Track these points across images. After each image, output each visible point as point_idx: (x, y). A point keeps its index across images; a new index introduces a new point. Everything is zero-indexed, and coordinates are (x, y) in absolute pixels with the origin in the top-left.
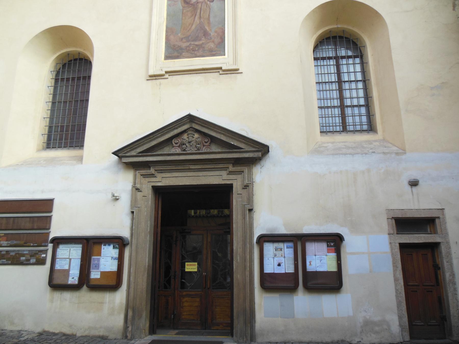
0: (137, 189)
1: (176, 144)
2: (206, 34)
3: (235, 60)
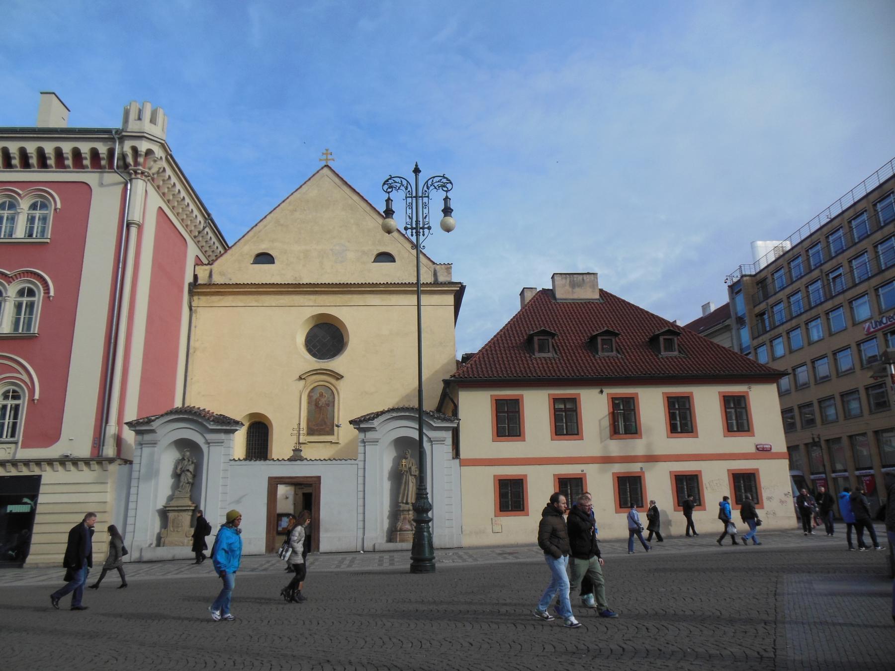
0: (297, 494)
2: (325, 423)
3: (338, 439)
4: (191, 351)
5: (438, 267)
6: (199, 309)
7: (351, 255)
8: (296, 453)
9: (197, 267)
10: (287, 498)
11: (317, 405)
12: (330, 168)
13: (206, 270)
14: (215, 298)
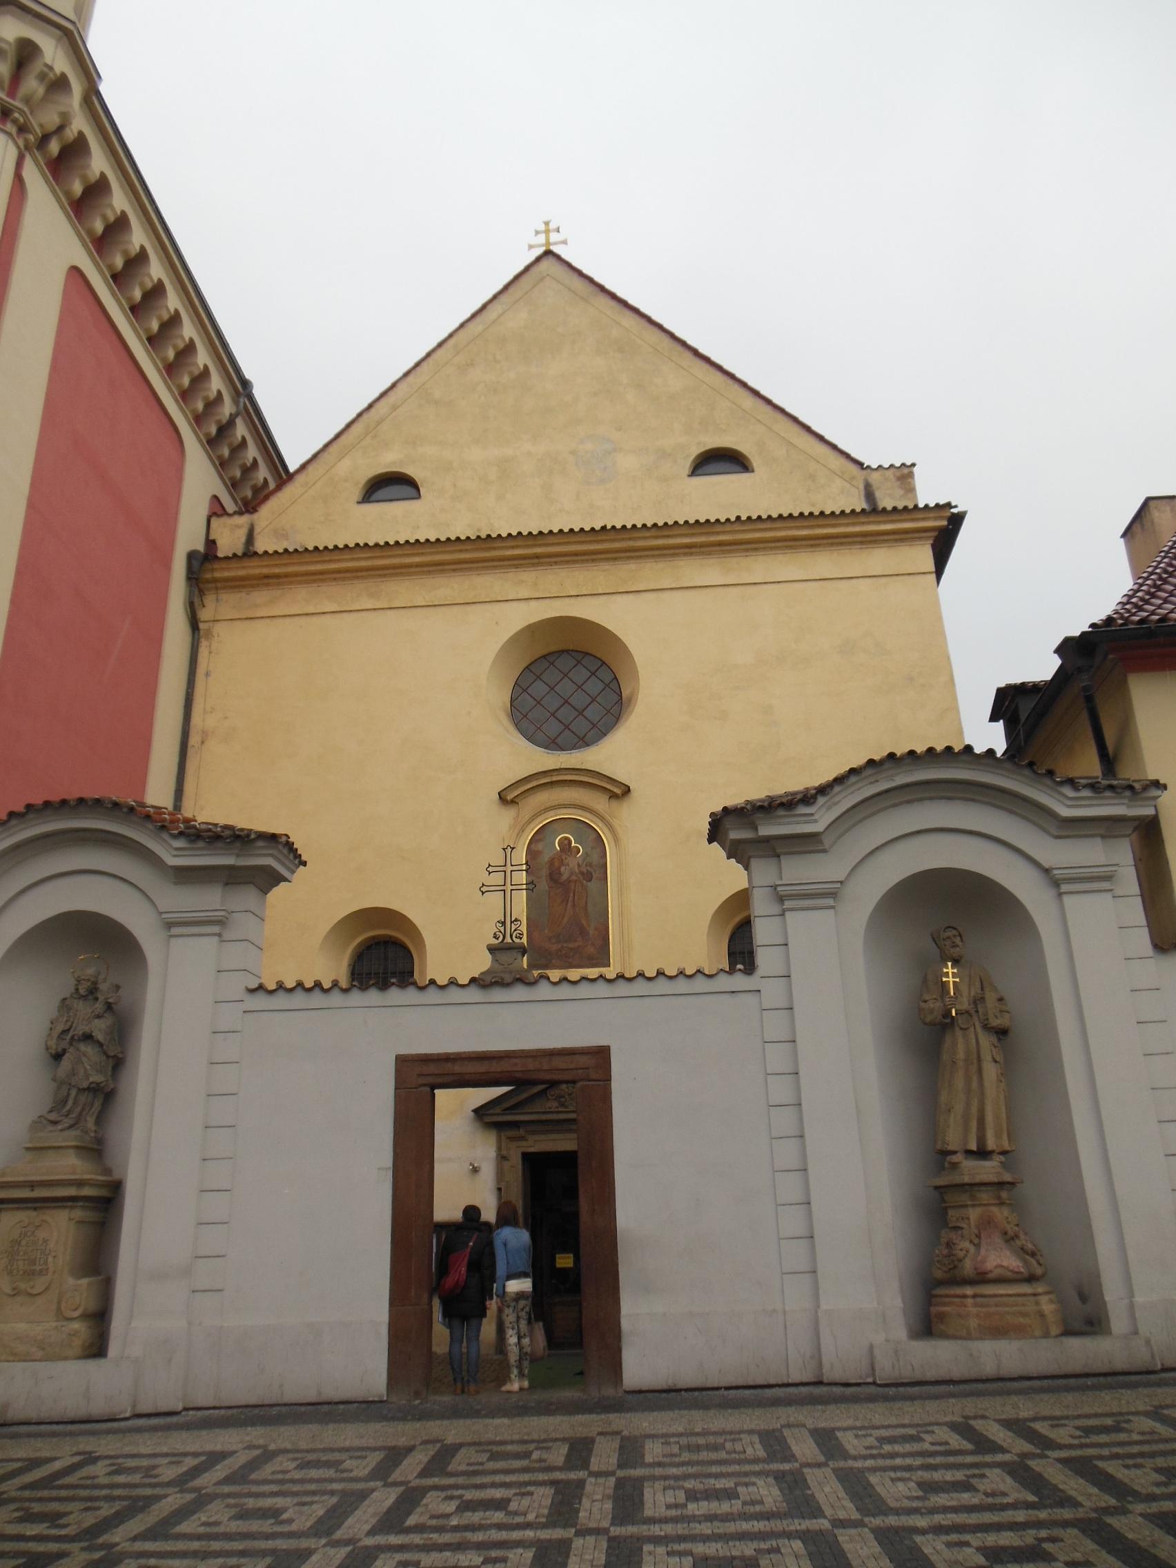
1: (553, 1096)
2: (583, 932)
4: (194, 740)
5: (875, 478)
7: (627, 463)
8: (505, 957)
9: (214, 521)
10: (475, 1170)
11: (554, 876)
12: (558, 257)
14: (260, 596)
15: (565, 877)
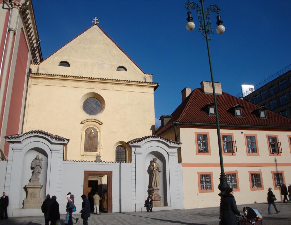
2: (93, 146)
4: (27, 106)
6: (32, 86)
8: (98, 158)
11: (89, 136)
13: (36, 67)
15: (91, 137)
